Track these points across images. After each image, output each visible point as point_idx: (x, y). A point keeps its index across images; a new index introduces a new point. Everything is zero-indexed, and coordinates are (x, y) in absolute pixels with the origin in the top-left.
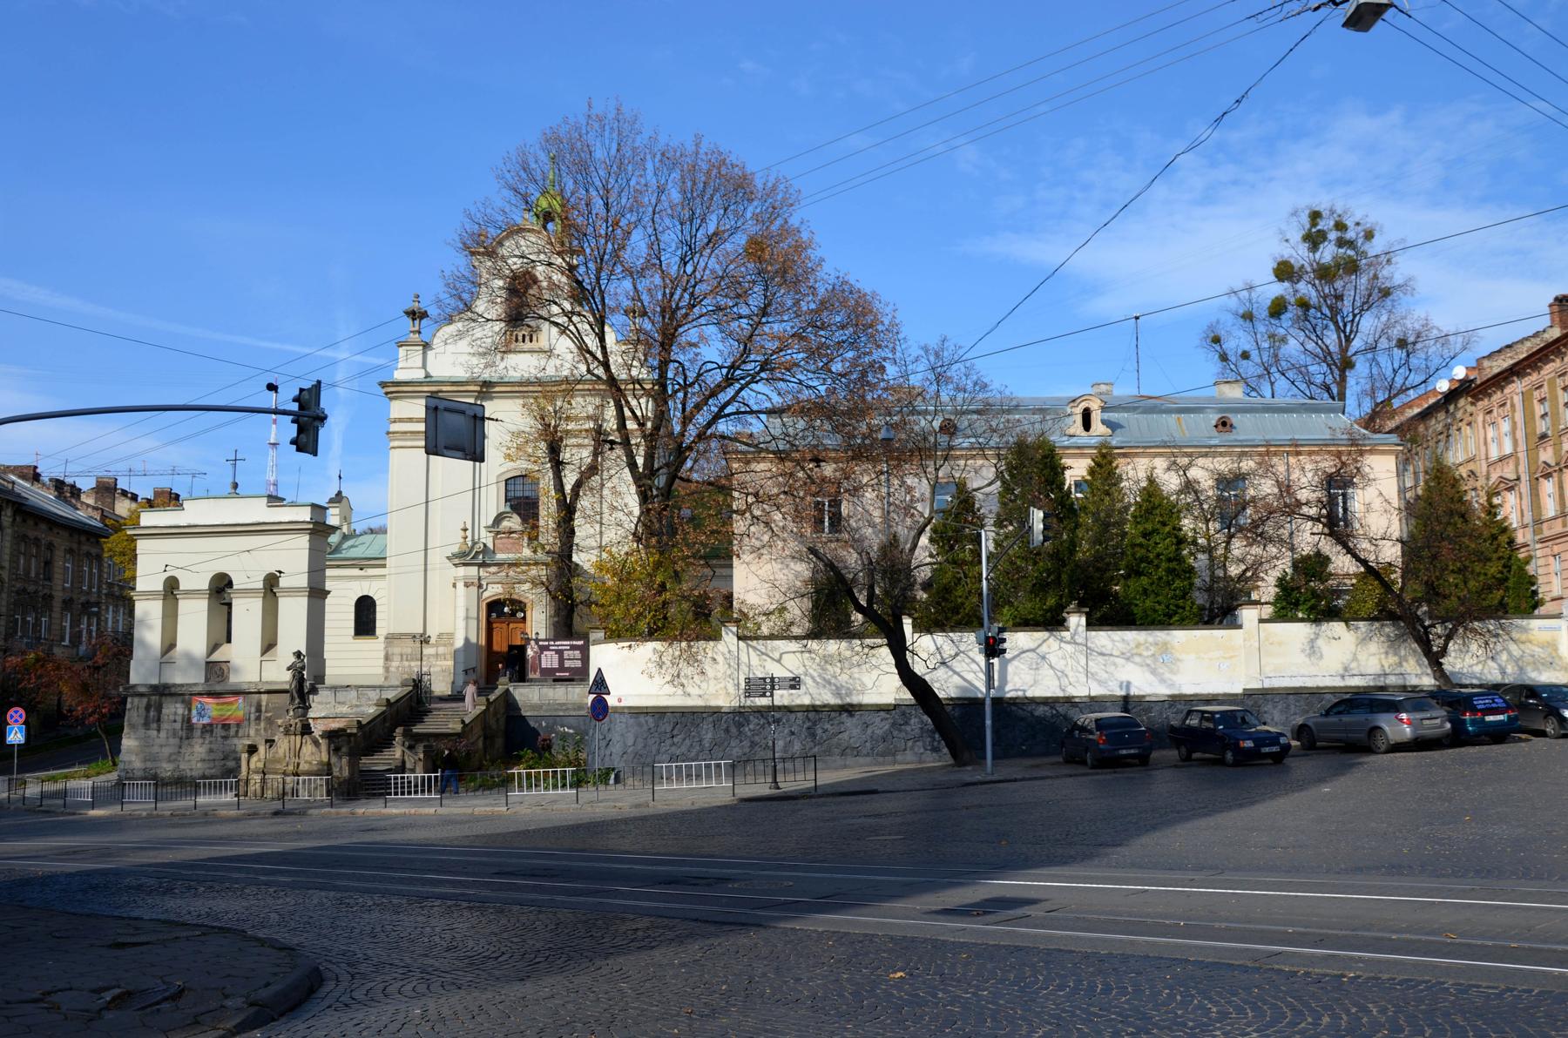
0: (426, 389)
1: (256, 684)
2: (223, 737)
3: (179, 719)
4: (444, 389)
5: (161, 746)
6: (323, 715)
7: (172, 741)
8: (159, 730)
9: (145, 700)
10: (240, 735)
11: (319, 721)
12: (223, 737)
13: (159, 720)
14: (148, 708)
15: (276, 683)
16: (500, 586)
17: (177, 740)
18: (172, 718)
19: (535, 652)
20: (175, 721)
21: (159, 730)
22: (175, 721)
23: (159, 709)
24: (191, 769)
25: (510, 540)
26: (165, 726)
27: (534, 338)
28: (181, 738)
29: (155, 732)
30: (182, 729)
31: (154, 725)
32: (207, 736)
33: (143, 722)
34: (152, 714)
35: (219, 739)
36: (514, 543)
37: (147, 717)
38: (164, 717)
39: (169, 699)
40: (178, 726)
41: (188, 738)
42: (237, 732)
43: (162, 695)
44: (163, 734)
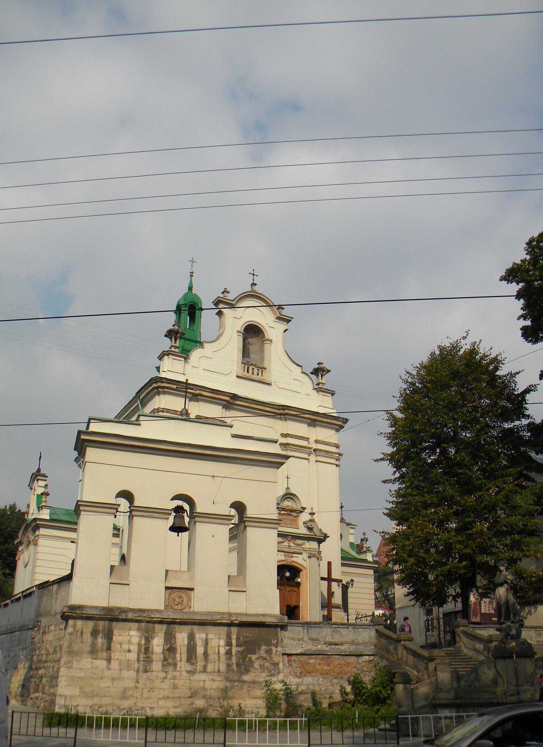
2: (188, 672)
3: (134, 648)
4: (204, 393)
5: (113, 679)
6: (299, 651)
7: (126, 673)
8: (109, 660)
9: (90, 624)
10: (210, 668)
11: (293, 658)
12: (188, 672)
13: (109, 648)
14: (95, 633)
15: (246, 615)
16: (283, 554)
17: (133, 673)
18: (126, 647)
19: (476, 599)
20: (129, 651)
22: (129, 651)
23: (109, 637)
24: (151, 708)
25: (290, 518)
26: (115, 655)
27: (260, 373)
28: (138, 671)
29: (104, 663)
30: (138, 661)
31: (104, 654)
32: (170, 669)
33: (89, 649)
35: (184, 674)
36: (293, 520)
37: (93, 645)
38: (115, 646)
39: (121, 624)
40: (133, 656)
41: (146, 671)
42: (205, 667)
43: (112, 620)
44: (115, 665)
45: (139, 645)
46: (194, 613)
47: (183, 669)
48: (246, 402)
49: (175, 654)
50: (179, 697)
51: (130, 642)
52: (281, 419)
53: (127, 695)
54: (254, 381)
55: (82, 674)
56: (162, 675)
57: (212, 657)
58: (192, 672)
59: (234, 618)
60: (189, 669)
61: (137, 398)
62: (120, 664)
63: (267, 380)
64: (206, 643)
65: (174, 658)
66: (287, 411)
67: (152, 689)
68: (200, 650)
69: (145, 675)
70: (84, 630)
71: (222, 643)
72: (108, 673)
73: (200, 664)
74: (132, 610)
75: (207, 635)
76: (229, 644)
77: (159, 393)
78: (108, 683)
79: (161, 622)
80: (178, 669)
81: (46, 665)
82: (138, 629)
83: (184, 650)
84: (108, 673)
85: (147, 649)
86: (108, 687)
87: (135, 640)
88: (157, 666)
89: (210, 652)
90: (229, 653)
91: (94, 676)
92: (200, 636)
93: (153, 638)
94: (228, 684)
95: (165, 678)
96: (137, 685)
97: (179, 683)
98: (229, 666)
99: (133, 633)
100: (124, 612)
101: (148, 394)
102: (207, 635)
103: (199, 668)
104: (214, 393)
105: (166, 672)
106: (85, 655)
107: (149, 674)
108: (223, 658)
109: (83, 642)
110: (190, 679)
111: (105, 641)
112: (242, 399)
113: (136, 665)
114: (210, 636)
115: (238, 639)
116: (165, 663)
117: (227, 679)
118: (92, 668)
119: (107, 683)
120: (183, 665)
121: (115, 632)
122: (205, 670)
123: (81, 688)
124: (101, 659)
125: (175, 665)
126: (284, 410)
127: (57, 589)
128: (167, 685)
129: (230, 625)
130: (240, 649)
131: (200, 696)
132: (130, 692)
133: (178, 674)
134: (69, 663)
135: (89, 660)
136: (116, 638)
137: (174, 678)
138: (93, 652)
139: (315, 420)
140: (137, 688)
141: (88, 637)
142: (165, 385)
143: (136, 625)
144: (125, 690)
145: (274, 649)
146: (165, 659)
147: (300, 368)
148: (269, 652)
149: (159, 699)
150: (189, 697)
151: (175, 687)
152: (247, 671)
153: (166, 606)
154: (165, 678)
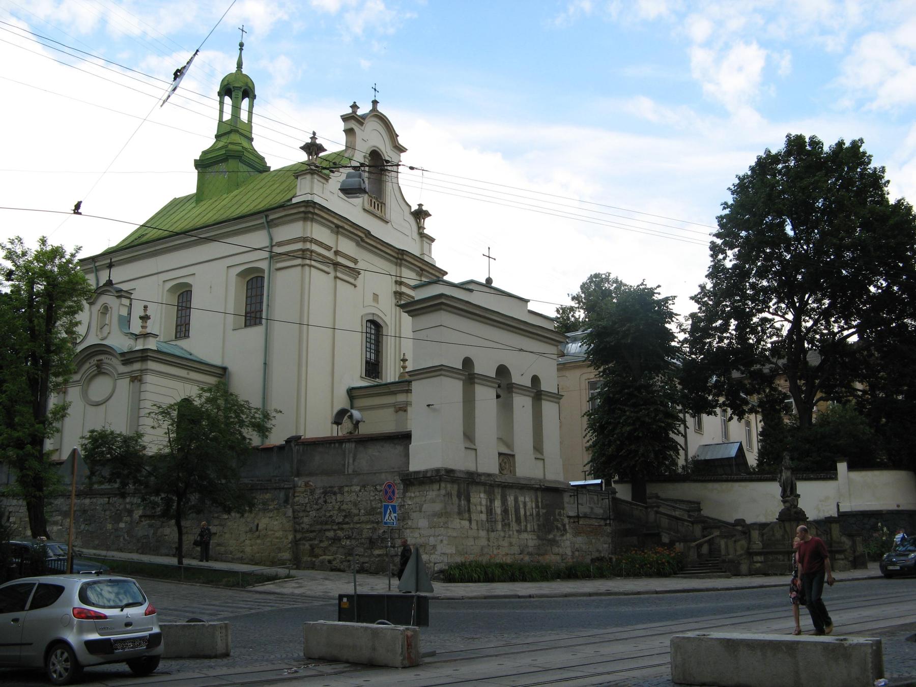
0: (336, 221)
1: (540, 480)
3: (484, 509)
4: (346, 227)
5: (475, 538)
8: (470, 521)
10: (529, 529)
12: (517, 531)
13: (469, 511)
14: (459, 497)
18: (479, 508)
20: (481, 512)
21: (470, 521)
26: (474, 517)
28: (488, 531)
29: (466, 523)
31: (466, 515)
33: (456, 510)
34: (463, 502)
35: (515, 533)
37: (459, 506)
38: (473, 508)
40: (483, 517)
41: (493, 531)
42: (526, 526)
44: (474, 525)
45: (487, 506)
46: (520, 478)
47: (514, 529)
48: (374, 241)
49: (508, 514)
50: (514, 554)
51: (481, 504)
52: (396, 264)
53: (484, 553)
54: (376, 216)
55: (455, 534)
56: (502, 534)
57: (530, 518)
58: (519, 532)
59: (542, 484)
60: (517, 529)
61: (263, 215)
62: (477, 524)
63: (388, 217)
64: (525, 504)
65: (509, 520)
66: (405, 257)
67: (498, 547)
68: (522, 512)
69: (492, 535)
70: (452, 492)
71: (534, 506)
72: (471, 533)
73: (523, 524)
74: (484, 474)
75: (525, 498)
76: (537, 506)
77: (305, 219)
78: (470, 542)
79: (498, 486)
80: (511, 529)
81: (344, 526)
82: (485, 492)
83: (513, 512)
84: (471, 533)
85: (491, 510)
86: (472, 546)
87: (484, 502)
88: (499, 526)
89: (528, 514)
90: (538, 514)
91: (463, 536)
92: (521, 499)
93: (494, 500)
94: (540, 542)
95: (505, 537)
96: (489, 544)
97: (514, 541)
98: (539, 525)
99: (482, 495)
100: (480, 475)
101: (286, 216)
102: (525, 498)
103: (523, 528)
104: (354, 228)
105: (505, 531)
106: (455, 516)
107: (495, 533)
108: (535, 520)
109: (452, 504)
110: (518, 538)
111: (466, 503)
112: (372, 238)
113: (487, 525)
114: (527, 499)
115: (542, 502)
116: (503, 523)
117: (538, 537)
118: (461, 528)
119: (470, 542)
120: (514, 526)
121: (472, 495)
122: (526, 531)
123: (456, 547)
124: (465, 520)
125: (509, 525)
126: (402, 255)
127: (355, 446)
128: (505, 544)
129: (537, 489)
130: (544, 511)
131: (526, 553)
132: (486, 550)
133: (511, 533)
134: (446, 523)
135: (458, 520)
136: (472, 500)
137: (510, 537)
138: (460, 513)
139: (422, 270)
140: (489, 546)
141: (455, 499)
142: (317, 211)
143: (482, 489)
144: (482, 548)
145: (562, 511)
146: (503, 520)
147: (408, 207)
148: (560, 514)
149: (503, 555)
150: (521, 554)
151: (511, 544)
152: (549, 532)
153: (500, 472)
154: (505, 537)
